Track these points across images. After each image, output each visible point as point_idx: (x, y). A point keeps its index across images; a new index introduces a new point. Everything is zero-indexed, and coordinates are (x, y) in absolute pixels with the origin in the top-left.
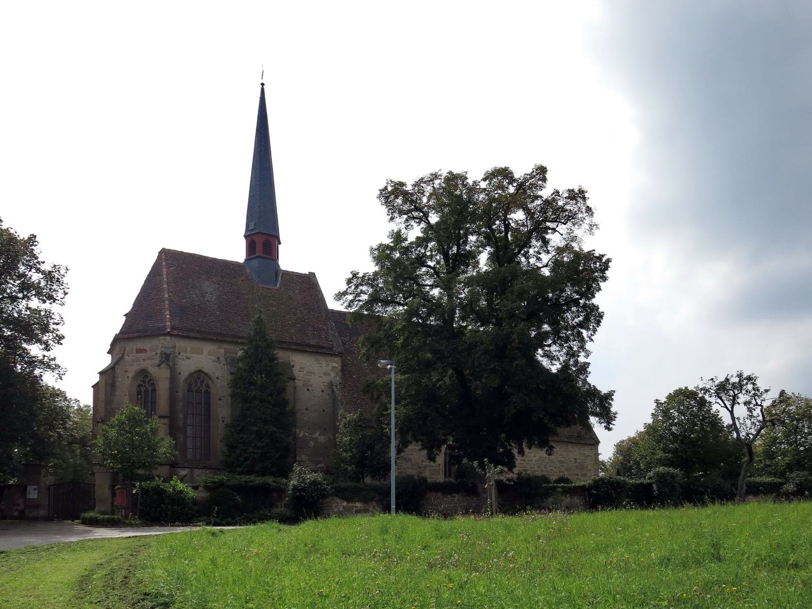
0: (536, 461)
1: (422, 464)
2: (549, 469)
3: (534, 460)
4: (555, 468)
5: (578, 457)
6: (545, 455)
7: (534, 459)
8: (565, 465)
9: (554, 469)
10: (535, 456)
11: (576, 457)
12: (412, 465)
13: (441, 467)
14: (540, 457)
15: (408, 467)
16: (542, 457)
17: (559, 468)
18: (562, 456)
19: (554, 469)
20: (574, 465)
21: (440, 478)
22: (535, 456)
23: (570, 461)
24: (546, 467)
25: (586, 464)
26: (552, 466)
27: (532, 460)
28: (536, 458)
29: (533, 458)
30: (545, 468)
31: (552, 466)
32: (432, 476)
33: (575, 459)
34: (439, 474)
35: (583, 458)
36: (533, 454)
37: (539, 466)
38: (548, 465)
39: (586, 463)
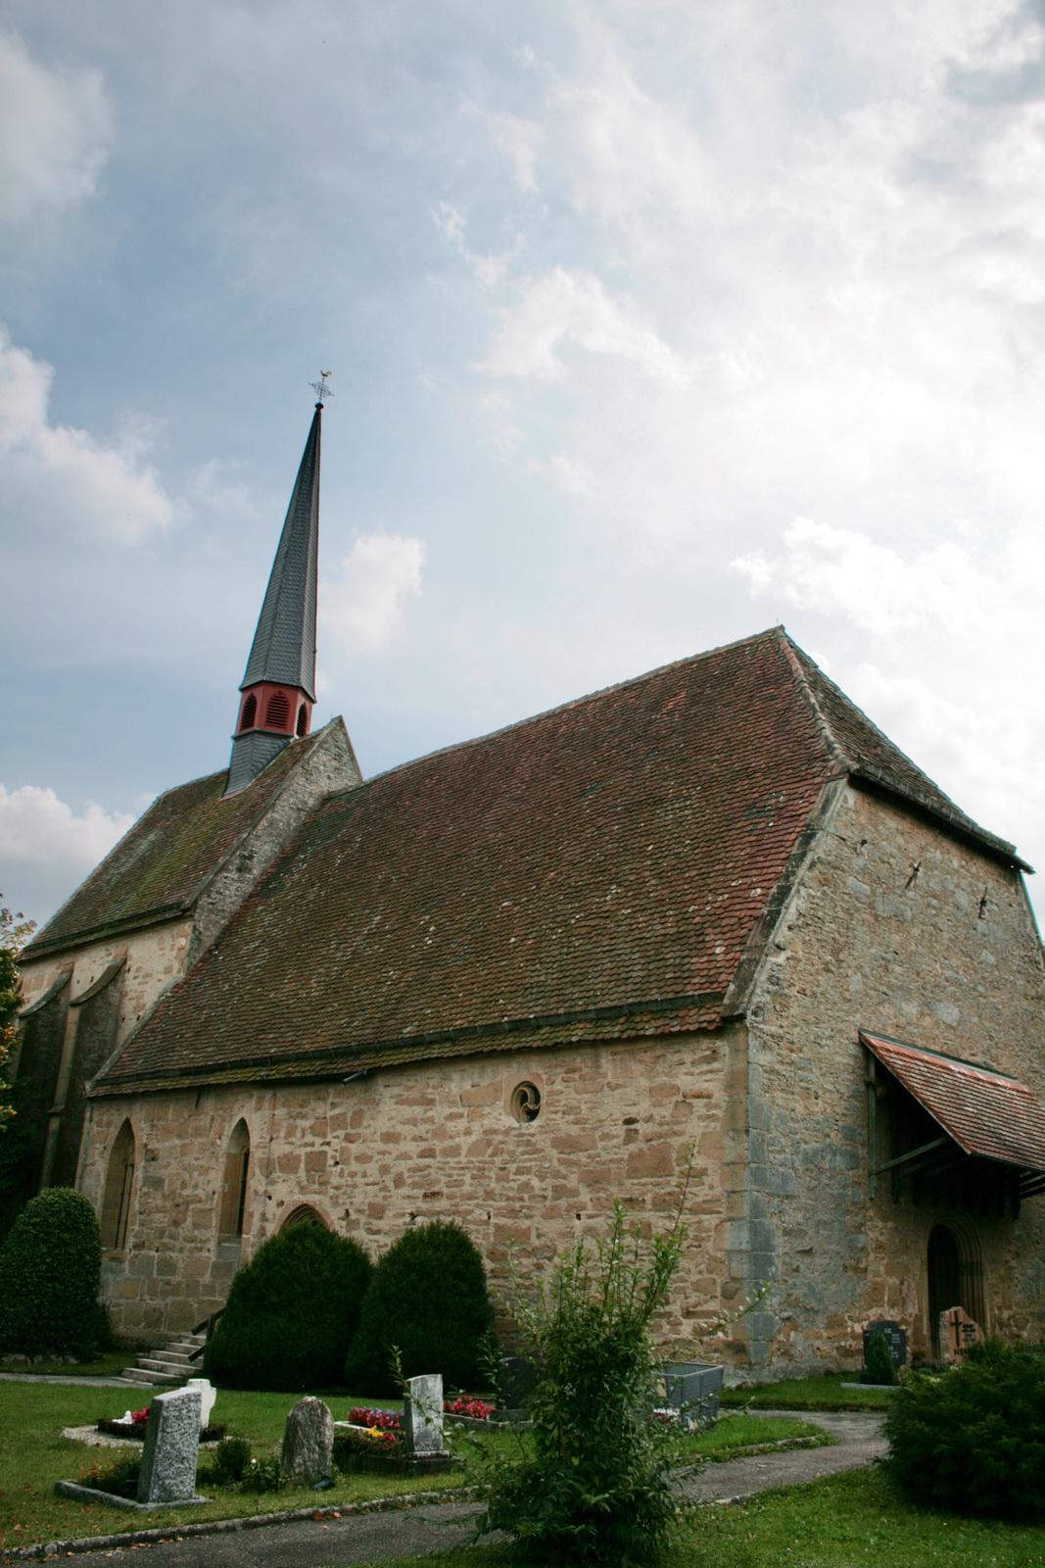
0: (470, 1152)
1: (180, 1195)
2: (514, 1185)
3: (464, 1152)
4: (542, 1178)
5: (643, 1108)
6: (511, 1122)
7: (465, 1142)
8: (582, 1157)
9: (536, 1182)
10: (468, 1133)
11: (633, 1112)
12: (165, 1197)
13: (215, 1203)
14: (485, 1132)
15: (157, 1207)
16: (495, 1132)
17: (556, 1175)
18: (571, 1118)
19: (536, 1182)
20: (624, 1153)
21: (209, 1240)
22: (468, 1133)
23: (606, 1137)
24: (503, 1175)
25: (676, 1142)
26: (528, 1171)
27: (455, 1151)
28: (473, 1138)
29: (461, 1140)
30: (499, 1180)
31: (528, 1171)
32: (196, 1232)
33: (629, 1121)
34: (207, 1227)
35: (666, 1112)
36: (462, 1124)
37: (480, 1175)
38: (513, 1167)
39: (681, 1134)
